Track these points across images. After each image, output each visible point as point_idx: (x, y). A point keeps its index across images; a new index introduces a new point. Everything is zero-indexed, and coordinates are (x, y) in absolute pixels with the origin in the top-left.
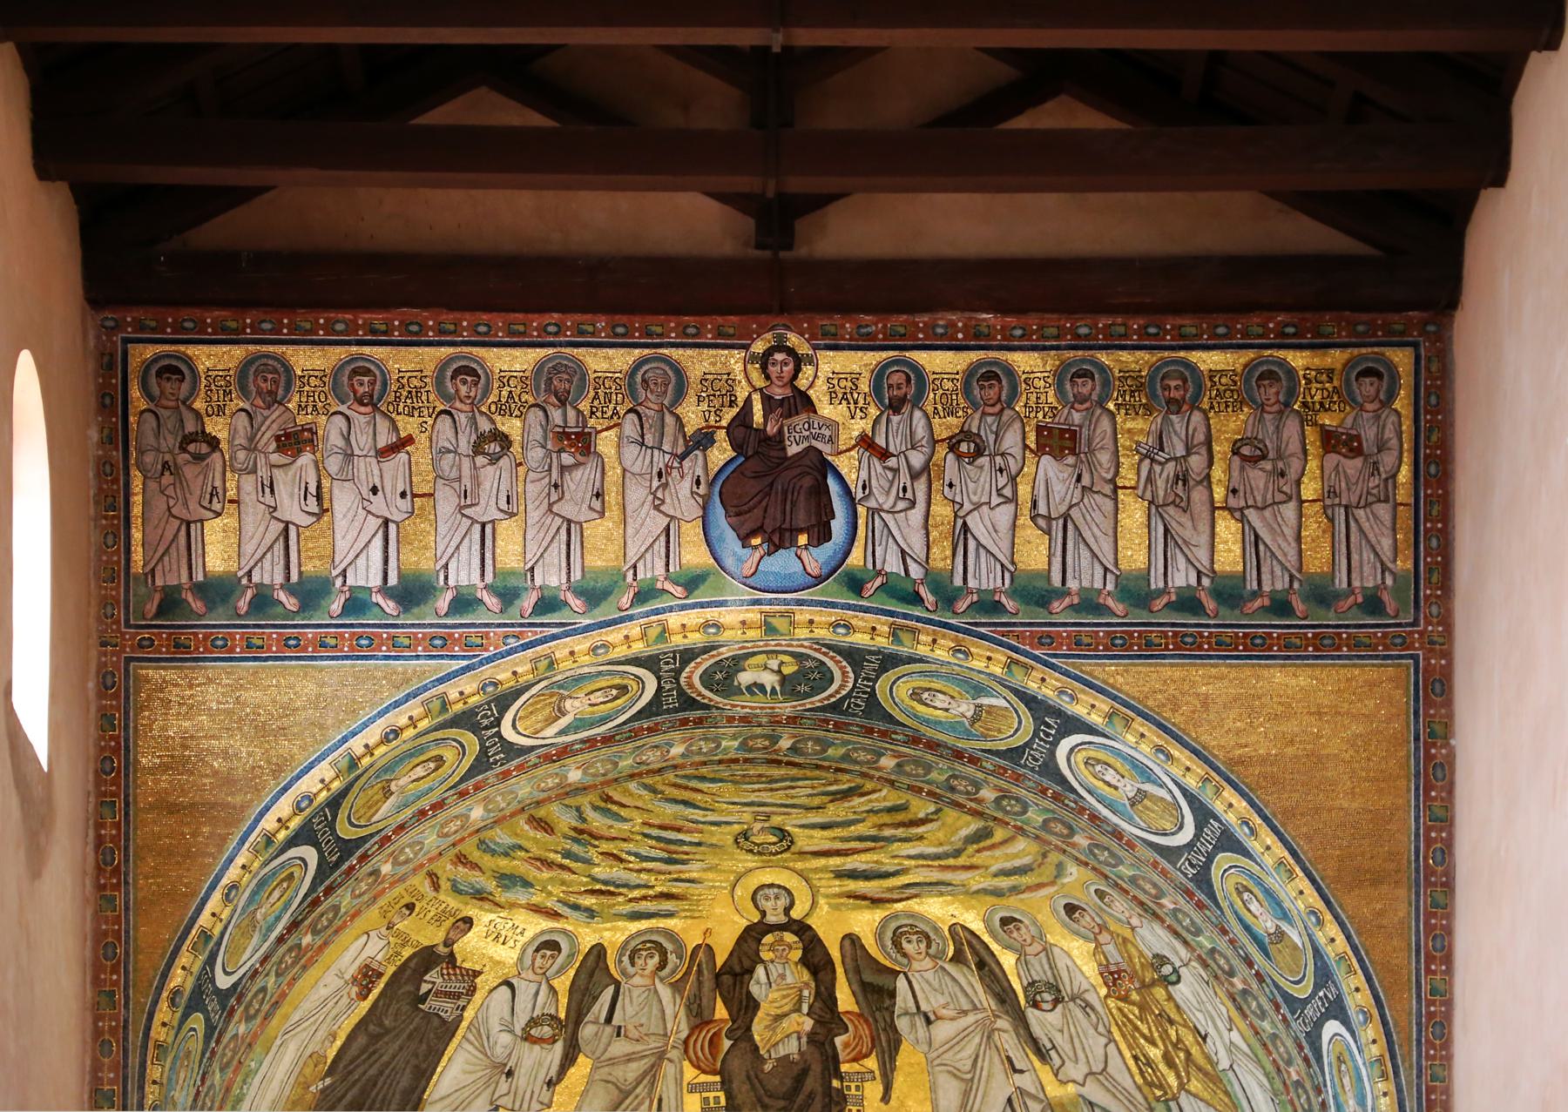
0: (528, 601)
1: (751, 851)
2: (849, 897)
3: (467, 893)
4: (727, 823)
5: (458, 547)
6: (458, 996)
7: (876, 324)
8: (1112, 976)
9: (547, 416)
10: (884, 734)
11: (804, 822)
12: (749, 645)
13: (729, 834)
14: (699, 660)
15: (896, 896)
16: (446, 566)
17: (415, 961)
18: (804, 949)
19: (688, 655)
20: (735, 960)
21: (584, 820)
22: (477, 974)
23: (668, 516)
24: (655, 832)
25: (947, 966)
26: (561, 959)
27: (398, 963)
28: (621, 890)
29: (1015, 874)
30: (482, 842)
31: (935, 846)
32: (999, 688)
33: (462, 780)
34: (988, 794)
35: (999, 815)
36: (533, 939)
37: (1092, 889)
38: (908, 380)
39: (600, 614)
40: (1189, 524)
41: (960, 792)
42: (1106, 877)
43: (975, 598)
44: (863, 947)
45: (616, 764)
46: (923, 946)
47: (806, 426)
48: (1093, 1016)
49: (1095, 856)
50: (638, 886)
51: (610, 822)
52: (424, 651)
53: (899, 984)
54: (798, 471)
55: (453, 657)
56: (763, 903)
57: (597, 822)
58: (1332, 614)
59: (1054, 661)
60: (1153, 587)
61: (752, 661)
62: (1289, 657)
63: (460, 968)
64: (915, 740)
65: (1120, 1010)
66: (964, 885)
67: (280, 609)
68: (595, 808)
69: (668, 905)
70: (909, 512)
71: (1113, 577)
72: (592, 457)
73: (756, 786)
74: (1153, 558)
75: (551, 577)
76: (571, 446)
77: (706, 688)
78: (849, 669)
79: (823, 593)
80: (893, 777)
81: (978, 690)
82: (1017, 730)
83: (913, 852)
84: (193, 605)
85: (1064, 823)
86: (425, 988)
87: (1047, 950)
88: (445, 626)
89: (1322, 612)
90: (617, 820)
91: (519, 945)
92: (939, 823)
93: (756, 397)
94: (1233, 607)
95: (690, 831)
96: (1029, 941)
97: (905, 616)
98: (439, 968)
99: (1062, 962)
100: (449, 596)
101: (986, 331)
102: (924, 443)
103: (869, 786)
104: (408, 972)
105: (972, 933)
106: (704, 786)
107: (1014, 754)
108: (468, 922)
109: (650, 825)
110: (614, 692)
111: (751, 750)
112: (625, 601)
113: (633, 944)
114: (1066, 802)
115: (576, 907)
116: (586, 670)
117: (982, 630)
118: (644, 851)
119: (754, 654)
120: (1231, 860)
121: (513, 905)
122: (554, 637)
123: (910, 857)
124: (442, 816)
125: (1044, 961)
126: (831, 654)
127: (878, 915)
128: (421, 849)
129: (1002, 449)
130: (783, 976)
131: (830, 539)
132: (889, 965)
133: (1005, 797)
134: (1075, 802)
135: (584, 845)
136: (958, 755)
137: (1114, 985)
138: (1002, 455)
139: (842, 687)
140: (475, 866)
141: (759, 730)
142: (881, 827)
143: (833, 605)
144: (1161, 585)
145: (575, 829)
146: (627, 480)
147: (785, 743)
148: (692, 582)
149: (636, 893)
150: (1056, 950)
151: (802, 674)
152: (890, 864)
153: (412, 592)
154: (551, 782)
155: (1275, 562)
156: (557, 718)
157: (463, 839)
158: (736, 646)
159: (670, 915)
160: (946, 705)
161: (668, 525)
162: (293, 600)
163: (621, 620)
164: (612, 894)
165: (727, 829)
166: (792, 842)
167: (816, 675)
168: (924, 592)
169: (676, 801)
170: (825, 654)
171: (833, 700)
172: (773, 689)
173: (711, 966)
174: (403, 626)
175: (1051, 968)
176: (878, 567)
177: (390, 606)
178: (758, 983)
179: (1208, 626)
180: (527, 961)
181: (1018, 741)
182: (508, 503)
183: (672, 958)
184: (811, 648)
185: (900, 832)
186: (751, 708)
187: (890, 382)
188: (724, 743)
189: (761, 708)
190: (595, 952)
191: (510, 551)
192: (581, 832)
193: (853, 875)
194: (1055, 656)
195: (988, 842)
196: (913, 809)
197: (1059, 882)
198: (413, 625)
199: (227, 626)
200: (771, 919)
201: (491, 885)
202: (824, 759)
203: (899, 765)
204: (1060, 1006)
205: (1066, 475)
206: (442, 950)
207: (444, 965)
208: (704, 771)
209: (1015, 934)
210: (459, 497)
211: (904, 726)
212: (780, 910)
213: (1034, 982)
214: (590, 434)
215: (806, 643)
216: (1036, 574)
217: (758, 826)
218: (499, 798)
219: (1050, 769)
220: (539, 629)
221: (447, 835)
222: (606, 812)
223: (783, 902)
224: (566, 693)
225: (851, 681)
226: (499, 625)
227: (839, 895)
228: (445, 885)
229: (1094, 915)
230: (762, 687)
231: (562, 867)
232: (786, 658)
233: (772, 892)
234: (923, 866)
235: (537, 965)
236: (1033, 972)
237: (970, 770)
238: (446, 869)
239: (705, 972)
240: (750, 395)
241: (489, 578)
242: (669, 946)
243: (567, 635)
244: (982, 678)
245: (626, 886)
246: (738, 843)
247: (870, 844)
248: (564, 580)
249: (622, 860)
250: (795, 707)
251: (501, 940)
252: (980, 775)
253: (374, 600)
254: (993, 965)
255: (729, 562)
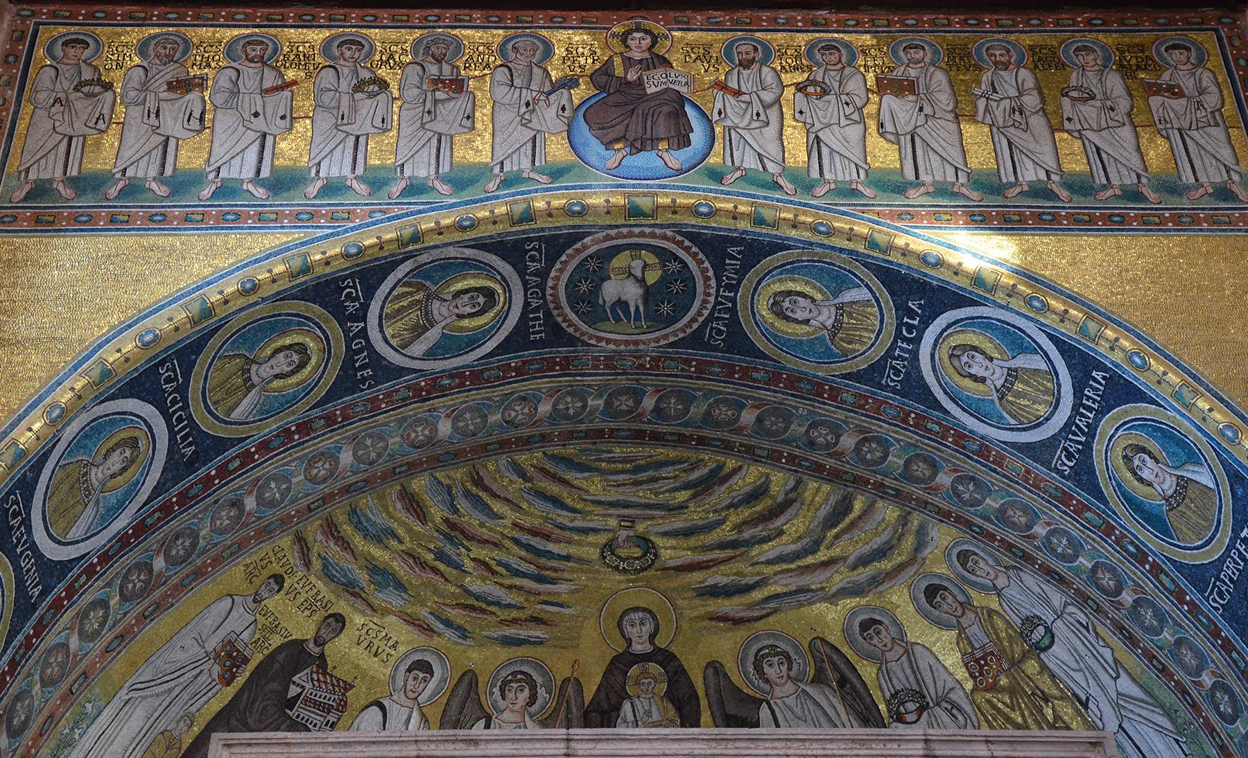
0: (396, 188)
1: (617, 568)
2: (711, 619)
3: (339, 582)
4: (595, 531)
5: (332, 151)
6: (327, 709)
7: (724, 17)
8: (976, 663)
9: (424, 69)
10: (745, 372)
11: (667, 528)
12: (613, 232)
13: (596, 545)
14: (564, 258)
15: (757, 614)
16: (319, 163)
17: (283, 655)
18: (669, 682)
19: (556, 245)
20: (603, 695)
21: (456, 511)
22: (348, 687)
23: (534, 130)
24: (525, 538)
25: (808, 689)
26: (432, 685)
27: (266, 652)
28: (492, 608)
29: (873, 560)
30: (354, 512)
31: (794, 542)
32: (862, 272)
33: (330, 397)
34: (848, 442)
35: (861, 471)
36: (406, 655)
37: (955, 551)
38: (756, 49)
39: (466, 196)
40: (1031, 139)
41: (820, 447)
42: (969, 524)
43: (833, 186)
44: (725, 674)
45: (484, 417)
46: (784, 668)
47: (664, 76)
48: (960, 718)
49: (959, 496)
50: (509, 606)
51: (484, 518)
52: (289, 222)
53: (761, 715)
54: (658, 102)
55: (317, 227)
56: (628, 629)
57: (471, 518)
58: (1185, 200)
59: (916, 230)
60: (1005, 181)
61: (619, 262)
62: (1151, 230)
63: (331, 676)
64: (774, 378)
65: (988, 701)
66: (822, 589)
67: (150, 195)
68: (468, 494)
69: (537, 632)
70: (763, 130)
71: (965, 174)
72: (464, 94)
73: (621, 477)
74: (1001, 162)
75: (422, 169)
76: (445, 87)
77: (572, 308)
78: (711, 273)
79: (684, 180)
80: (753, 442)
81: (838, 281)
82: (878, 335)
83: (771, 555)
84: (63, 193)
85: (925, 460)
86: (293, 691)
87: (909, 650)
88: (313, 205)
89: (1175, 199)
90: (487, 515)
91: (392, 660)
92: (797, 505)
93: (617, 60)
94: (1085, 195)
95: (558, 541)
96: (889, 645)
97: (765, 198)
98: (308, 671)
99: (923, 662)
100: (319, 184)
101: (823, 22)
102: (773, 86)
103: (731, 463)
104: (277, 666)
105: (834, 647)
106: (569, 476)
107: (872, 374)
108: (340, 619)
109: (522, 528)
110: (481, 300)
111: (617, 415)
112: (492, 186)
113: (504, 674)
114: (930, 425)
115: (448, 623)
116: (452, 252)
117: (842, 208)
118: (514, 563)
119: (618, 249)
120: (1115, 419)
121: (386, 612)
122: (420, 212)
123: (769, 562)
124: (309, 448)
125: (906, 665)
126: (694, 249)
127: (741, 634)
128: (288, 489)
129: (847, 91)
130: (648, 713)
131: (690, 145)
132: (751, 693)
133: (865, 439)
134: (938, 424)
135: (456, 545)
136: (818, 389)
137: (981, 674)
138: (847, 94)
139: (705, 302)
140: (347, 546)
141: (623, 381)
142: (739, 527)
143: (695, 189)
144: (1012, 179)
145: (446, 521)
146: (497, 109)
147: (649, 403)
148: (556, 173)
149: (504, 614)
150: (918, 649)
151: (664, 281)
152: (753, 575)
153: (283, 182)
154: (421, 433)
155: (1119, 165)
156: (425, 329)
157: (332, 496)
158: (601, 235)
159: (540, 643)
160: (806, 315)
161: (535, 136)
162: (164, 188)
163: (487, 199)
164: (483, 611)
165: (591, 538)
166: (656, 555)
167: (677, 287)
168: (780, 181)
169: (542, 495)
170: (687, 249)
171: (695, 326)
172: (637, 307)
173: (579, 699)
174: (271, 206)
175: (914, 672)
176: (737, 164)
177: (260, 192)
178: (625, 722)
179: (1064, 208)
180: (400, 683)
181: (877, 354)
182: (383, 122)
183: (541, 692)
184: (673, 240)
185: (758, 531)
186: (615, 342)
187: (739, 50)
188: (590, 402)
189: (627, 343)
190: (466, 679)
191: (379, 153)
192: (452, 525)
193: (714, 592)
194: (916, 227)
195: (847, 520)
196: (774, 489)
197: (920, 556)
198: (281, 205)
199: (96, 207)
200: (637, 648)
201: (363, 577)
202: (686, 425)
203: (759, 420)
204: (925, 713)
205: (908, 108)
206: (313, 649)
207: (315, 670)
208: (570, 450)
209: (875, 641)
210: (337, 119)
211: (765, 357)
212: (646, 637)
213: (897, 693)
214: (463, 80)
215: (669, 233)
216: (891, 171)
217: (623, 534)
218: (369, 442)
219: (915, 387)
220: (405, 207)
221: (313, 480)
222: (477, 502)
223: (648, 628)
224: (434, 288)
225: (713, 291)
226: (366, 204)
227: (701, 618)
228: (317, 564)
229: (956, 591)
230: (621, 304)
231: (435, 570)
232: (651, 259)
233: (636, 616)
234: (782, 572)
235: (408, 688)
236: (895, 681)
237: (828, 410)
238: (319, 543)
239: (574, 710)
240: (611, 57)
241: (360, 170)
242: (539, 680)
243: (433, 210)
244: (841, 260)
245: (498, 604)
246: (604, 558)
247: (729, 553)
248: (433, 172)
249: (494, 573)
250: (657, 340)
251: (374, 649)
252: (841, 415)
253: (245, 187)
254: (854, 680)
255: (593, 159)
